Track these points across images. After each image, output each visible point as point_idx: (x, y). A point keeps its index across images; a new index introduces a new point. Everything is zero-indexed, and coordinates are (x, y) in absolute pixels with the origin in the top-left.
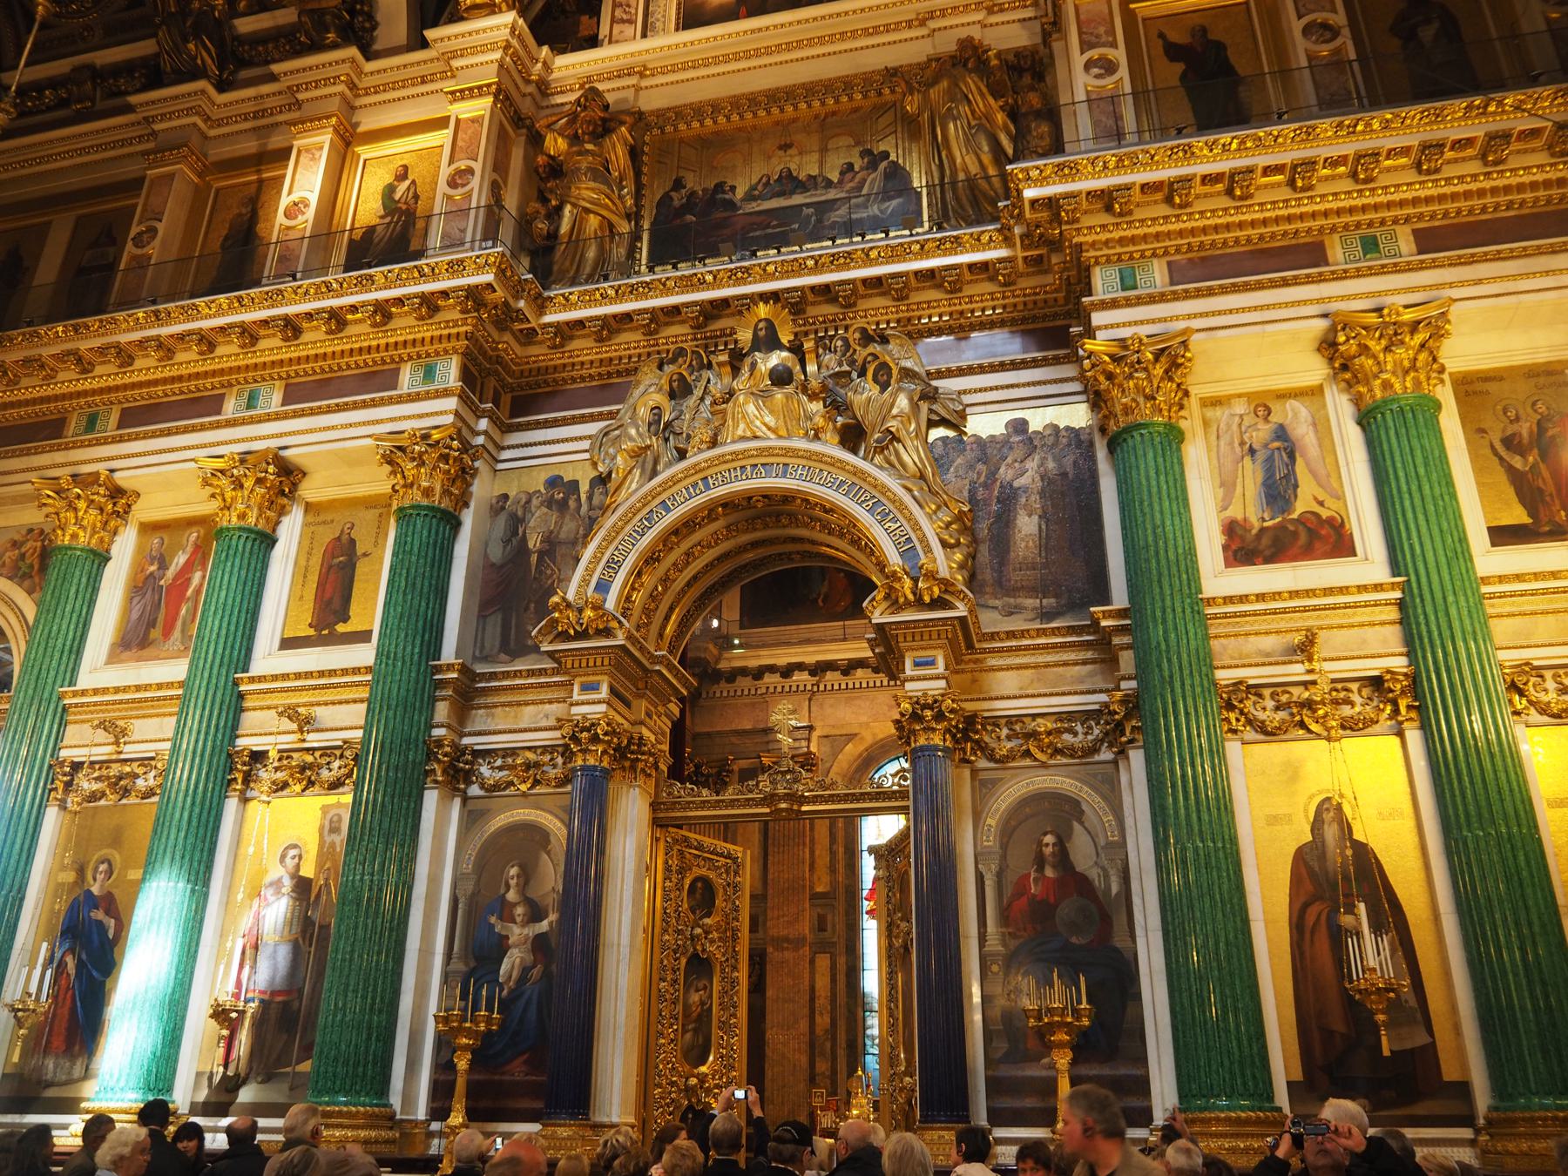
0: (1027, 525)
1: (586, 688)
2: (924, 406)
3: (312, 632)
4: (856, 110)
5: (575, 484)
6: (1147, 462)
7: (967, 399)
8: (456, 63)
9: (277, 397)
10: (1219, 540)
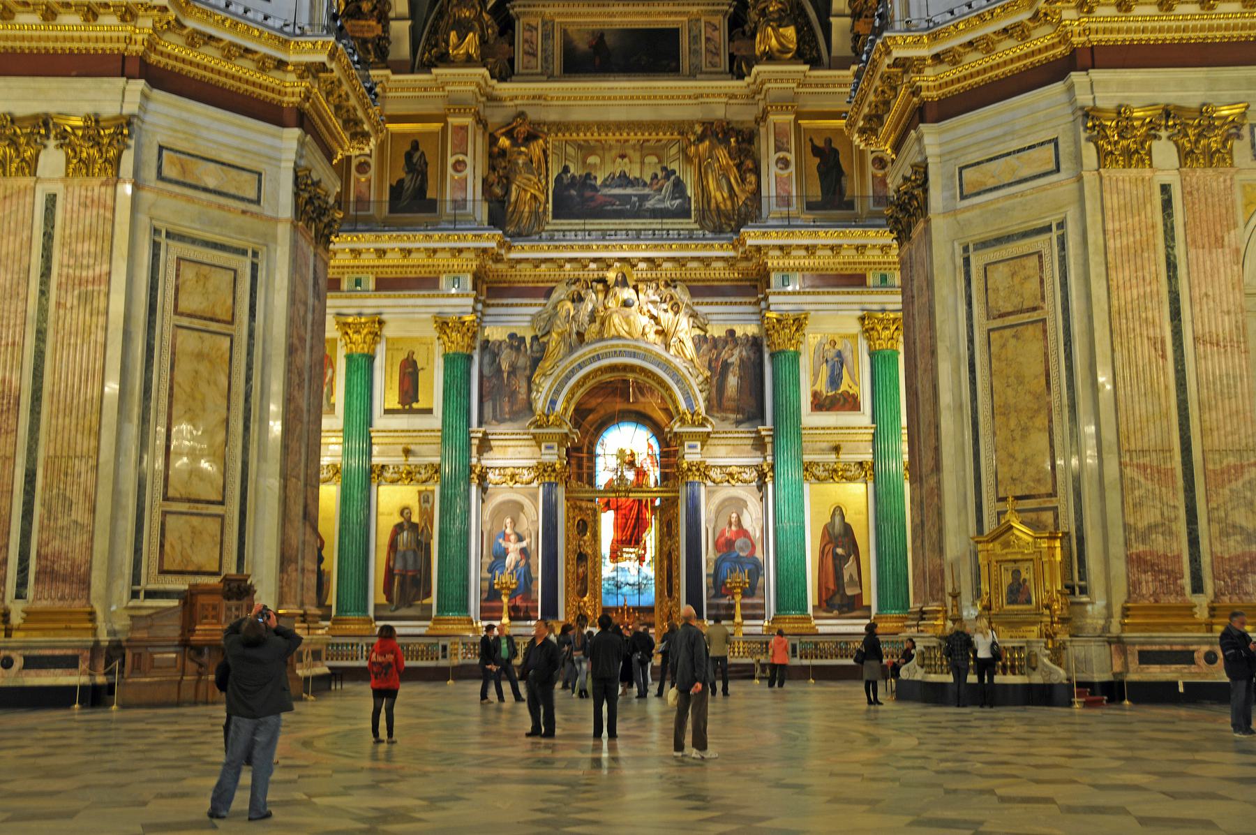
0: (732, 381)
1: (547, 448)
2: (691, 320)
3: (400, 406)
4: (659, 141)
5: (523, 339)
6: (785, 370)
7: (710, 317)
8: (447, 88)
9: (372, 285)
10: (810, 399)
